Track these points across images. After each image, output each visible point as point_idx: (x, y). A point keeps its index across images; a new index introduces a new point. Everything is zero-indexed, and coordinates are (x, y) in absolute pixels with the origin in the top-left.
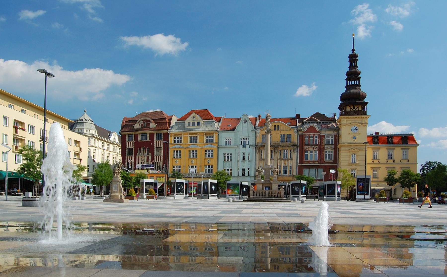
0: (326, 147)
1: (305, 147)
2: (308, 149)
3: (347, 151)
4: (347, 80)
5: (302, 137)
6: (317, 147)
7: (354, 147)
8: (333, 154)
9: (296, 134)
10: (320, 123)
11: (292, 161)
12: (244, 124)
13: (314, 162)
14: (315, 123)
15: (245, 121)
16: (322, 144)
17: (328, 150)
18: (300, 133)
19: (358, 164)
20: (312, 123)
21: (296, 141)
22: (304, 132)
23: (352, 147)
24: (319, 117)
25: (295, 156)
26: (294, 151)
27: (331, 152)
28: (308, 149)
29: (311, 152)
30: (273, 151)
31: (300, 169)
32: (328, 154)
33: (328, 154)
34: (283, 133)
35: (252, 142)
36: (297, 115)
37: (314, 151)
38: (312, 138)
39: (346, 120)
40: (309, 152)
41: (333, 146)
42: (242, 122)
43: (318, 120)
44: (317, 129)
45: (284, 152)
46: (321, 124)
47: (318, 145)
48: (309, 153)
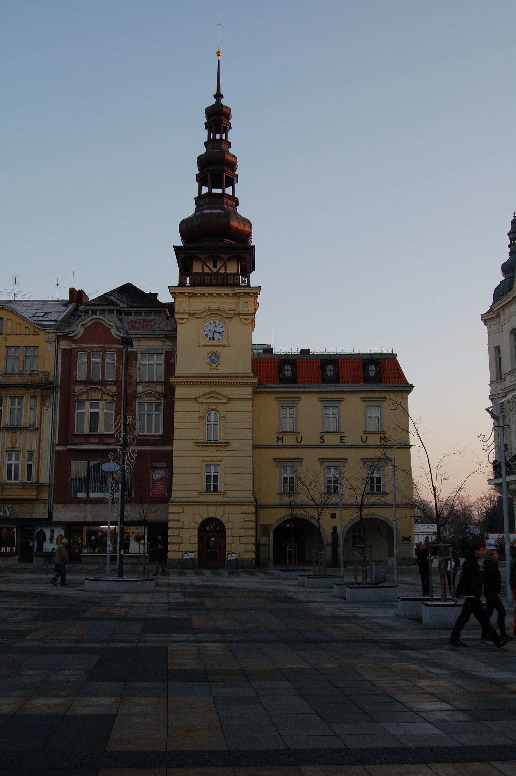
0: (140, 389)
1: (78, 388)
2: (84, 397)
3: (194, 403)
5: (69, 358)
6: (113, 389)
8: (161, 412)
9: (52, 348)
10: (128, 314)
11: (35, 436)
13: (102, 438)
14: (111, 312)
16: (128, 377)
17: (147, 400)
18: (64, 345)
19: (225, 444)
20: (102, 311)
21: (52, 370)
22: (75, 342)
24: (130, 298)
25: (48, 418)
26: (43, 404)
27: (157, 407)
28: (84, 397)
29: (94, 404)
31: (61, 461)
32: (146, 412)
33: (146, 412)
34: (12, 341)
36: (72, 291)
37: (102, 404)
38: (99, 360)
40: (87, 404)
41: (160, 389)
43: (123, 305)
44: (114, 332)
45: (13, 404)
46: (130, 318)
47: (114, 383)
48: (87, 409)
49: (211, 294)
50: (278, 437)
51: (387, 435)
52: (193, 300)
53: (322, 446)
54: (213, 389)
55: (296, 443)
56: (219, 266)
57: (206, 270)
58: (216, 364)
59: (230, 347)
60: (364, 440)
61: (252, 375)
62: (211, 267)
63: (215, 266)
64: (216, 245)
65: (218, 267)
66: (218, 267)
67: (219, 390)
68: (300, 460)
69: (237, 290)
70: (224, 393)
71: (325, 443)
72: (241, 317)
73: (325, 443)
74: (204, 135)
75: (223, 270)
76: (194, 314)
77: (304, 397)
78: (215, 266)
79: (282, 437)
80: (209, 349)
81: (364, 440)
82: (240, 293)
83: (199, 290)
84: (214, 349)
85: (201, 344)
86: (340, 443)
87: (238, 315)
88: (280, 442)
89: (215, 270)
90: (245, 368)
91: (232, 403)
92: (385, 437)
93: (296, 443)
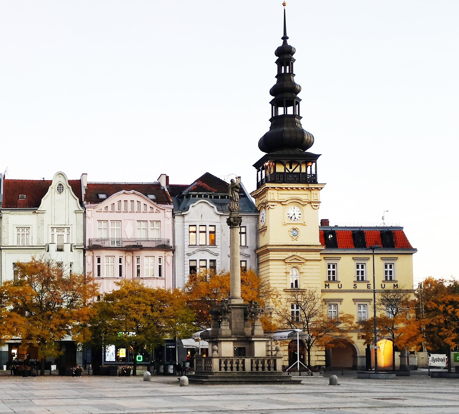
3: (282, 263)
4: (275, 104)
7: (295, 253)
12: (57, 196)
15: (60, 188)
23: (290, 254)
30: (123, 260)
35: (76, 238)
39: (273, 194)
42: (52, 190)
49: (292, 188)
50: (326, 285)
51: (398, 283)
52: (279, 192)
53: (355, 290)
54: (294, 253)
55: (337, 288)
56: (293, 167)
57: (287, 171)
58: (296, 237)
59: (305, 225)
60: (383, 287)
61: (320, 244)
62: (288, 167)
63: (291, 168)
64: (287, 149)
65: (293, 169)
66: (293, 168)
67: (298, 254)
68: (340, 300)
69: (311, 186)
70: (302, 256)
71: (357, 289)
72: (312, 204)
73: (357, 289)
74: (274, 69)
75: (297, 170)
76: (281, 202)
77: (344, 258)
78: (291, 168)
79: (329, 285)
80: (292, 226)
81: (383, 287)
82: (312, 188)
83: (284, 185)
84: (295, 227)
85: (286, 223)
86: (367, 289)
87: (310, 203)
88: (327, 288)
89: (291, 170)
90: (314, 238)
91: (308, 263)
92: (397, 285)
93: (337, 288)
